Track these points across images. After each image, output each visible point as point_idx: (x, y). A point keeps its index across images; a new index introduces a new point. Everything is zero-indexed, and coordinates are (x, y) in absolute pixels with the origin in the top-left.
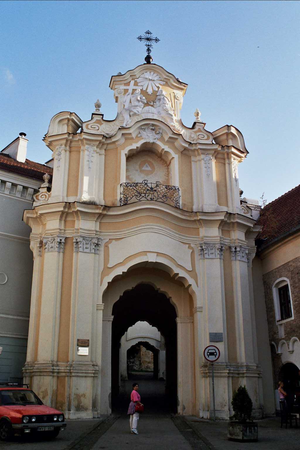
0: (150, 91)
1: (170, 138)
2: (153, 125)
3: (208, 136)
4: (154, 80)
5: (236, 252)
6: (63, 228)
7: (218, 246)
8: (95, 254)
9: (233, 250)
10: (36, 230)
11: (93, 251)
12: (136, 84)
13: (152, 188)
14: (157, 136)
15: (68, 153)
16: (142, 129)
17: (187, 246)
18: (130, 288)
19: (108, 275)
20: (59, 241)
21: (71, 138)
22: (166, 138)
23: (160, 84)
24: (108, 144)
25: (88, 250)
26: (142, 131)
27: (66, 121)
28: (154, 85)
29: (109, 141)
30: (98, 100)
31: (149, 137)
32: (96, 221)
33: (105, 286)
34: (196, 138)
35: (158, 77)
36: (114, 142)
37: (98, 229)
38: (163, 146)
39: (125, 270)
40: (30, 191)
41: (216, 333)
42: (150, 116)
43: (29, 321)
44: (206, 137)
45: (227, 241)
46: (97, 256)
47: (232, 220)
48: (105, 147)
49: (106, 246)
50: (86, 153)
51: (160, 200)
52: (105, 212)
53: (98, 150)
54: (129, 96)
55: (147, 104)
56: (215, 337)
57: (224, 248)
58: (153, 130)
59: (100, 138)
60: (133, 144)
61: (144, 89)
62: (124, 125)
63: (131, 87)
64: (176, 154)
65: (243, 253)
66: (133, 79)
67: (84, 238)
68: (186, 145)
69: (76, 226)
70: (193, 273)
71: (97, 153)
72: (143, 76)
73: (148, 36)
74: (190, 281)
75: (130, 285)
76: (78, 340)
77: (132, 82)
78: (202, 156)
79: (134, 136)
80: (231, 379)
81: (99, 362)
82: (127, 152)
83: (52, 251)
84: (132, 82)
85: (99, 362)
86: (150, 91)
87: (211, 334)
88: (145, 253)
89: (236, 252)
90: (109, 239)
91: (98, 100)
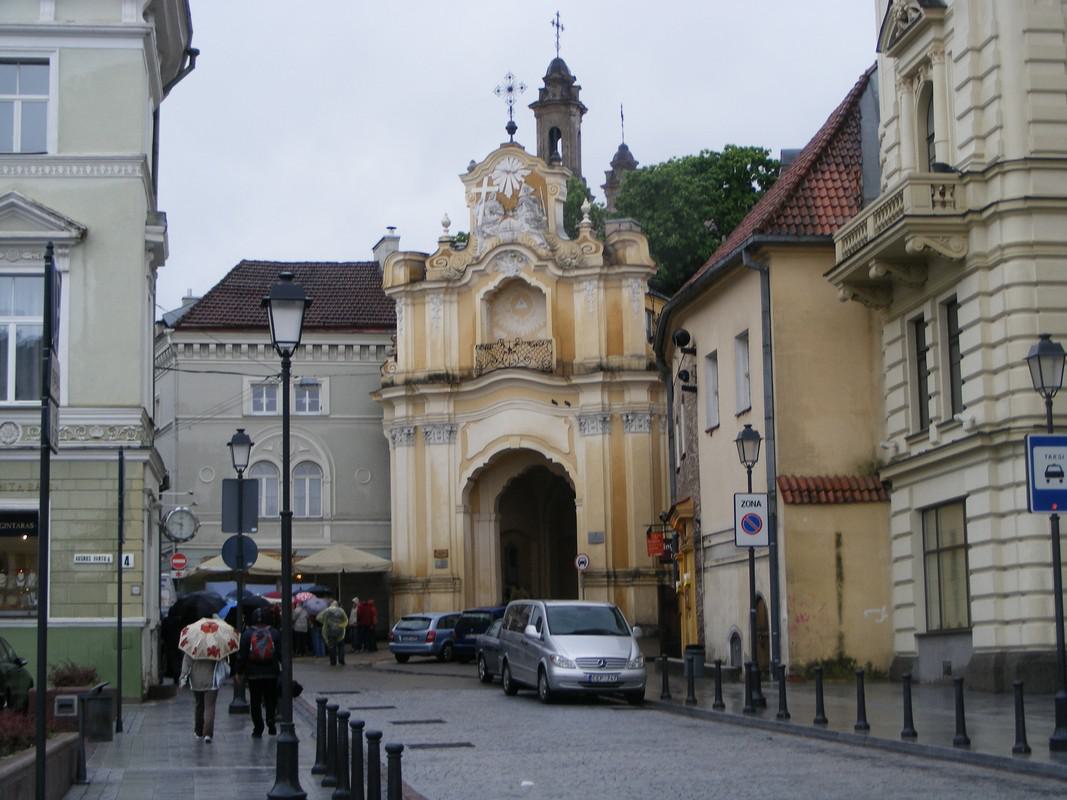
0: (509, 193)
1: (536, 266)
2: (512, 251)
3: (596, 245)
4: (514, 173)
5: (628, 420)
6: (410, 413)
7: (600, 418)
8: (449, 443)
9: (625, 418)
10: (387, 415)
11: (447, 441)
12: (490, 183)
13: (510, 349)
14: (521, 265)
15: (410, 308)
16: (500, 259)
17: (563, 420)
18: (516, 475)
19: (467, 468)
20: (406, 431)
21: (408, 289)
22: (533, 267)
23: (523, 176)
24: (460, 287)
25: (441, 441)
26: (499, 262)
27: (403, 263)
28: (509, 183)
29: (459, 284)
30: (446, 215)
31: (508, 269)
32: (449, 401)
33: (465, 482)
34: (579, 252)
35: (520, 164)
36: (466, 284)
37: (451, 410)
38: (533, 281)
39: (486, 461)
40: (388, 348)
41: (596, 533)
42: (507, 236)
43: (390, 526)
44: (594, 249)
45: (617, 407)
46: (452, 447)
47: (618, 379)
48: (456, 290)
49: (464, 433)
50: (431, 306)
51: (522, 364)
52: (456, 389)
53: (447, 298)
54: (483, 205)
55: (505, 216)
56: (595, 539)
57: (608, 419)
58: (515, 256)
59: (444, 285)
60: (490, 283)
61: (501, 191)
62: (478, 254)
63: (484, 189)
64: (547, 286)
65: (640, 420)
66: (486, 175)
67: (434, 426)
68: (560, 273)
69: (427, 411)
70: (569, 454)
71: (445, 301)
72: (498, 167)
73: (508, 83)
74: (568, 467)
75: (516, 470)
76: (435, 551)
77: (486, 180)
78: (585, 284)
79: (489, 271)
80: (612, 590)
81: (462, 575)
82: (482, 296)
83: (401, 446)
84: (486, 180)
85: (462, 575)
86: (509, 193)
87: (590, 535)
88: (508, 437)
89: (628, 420)
90: (468, 422)
91: (446, 215)
